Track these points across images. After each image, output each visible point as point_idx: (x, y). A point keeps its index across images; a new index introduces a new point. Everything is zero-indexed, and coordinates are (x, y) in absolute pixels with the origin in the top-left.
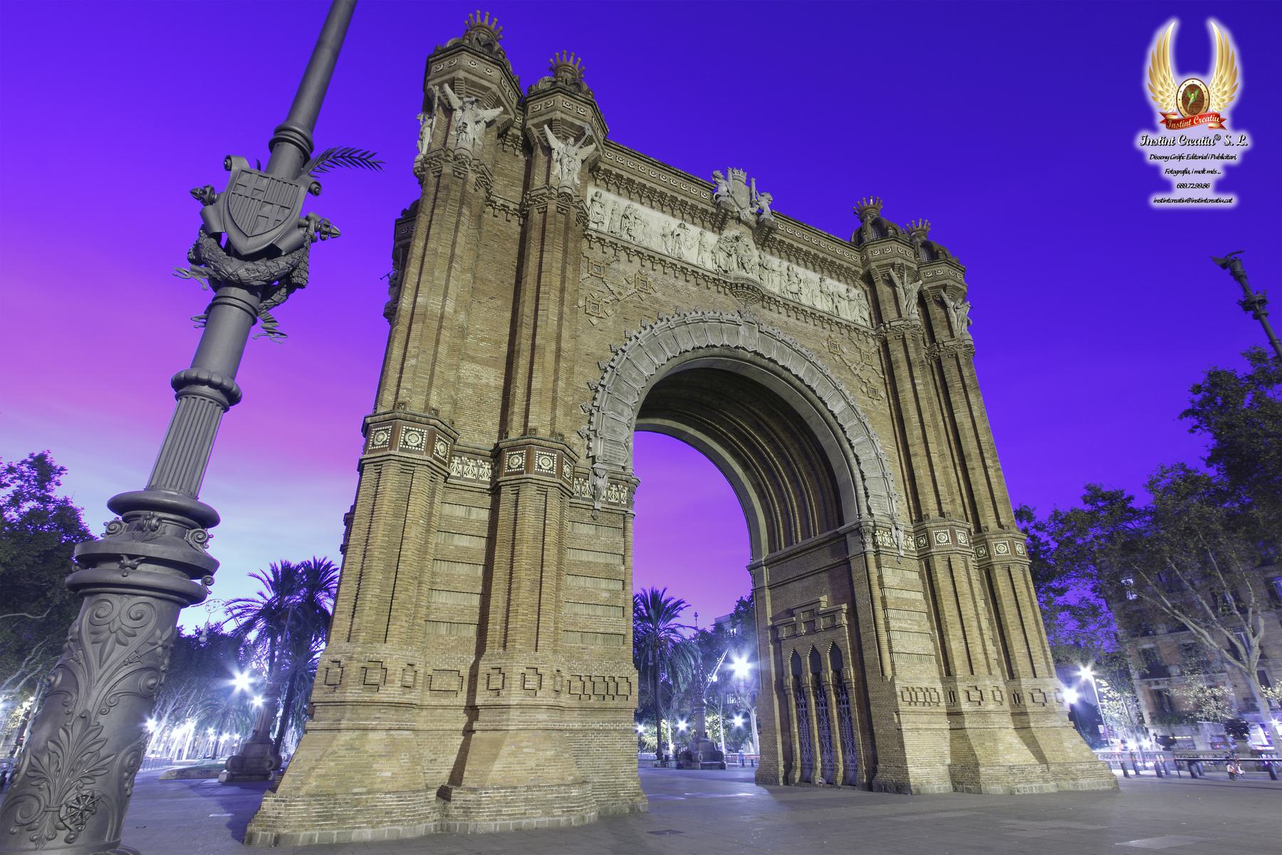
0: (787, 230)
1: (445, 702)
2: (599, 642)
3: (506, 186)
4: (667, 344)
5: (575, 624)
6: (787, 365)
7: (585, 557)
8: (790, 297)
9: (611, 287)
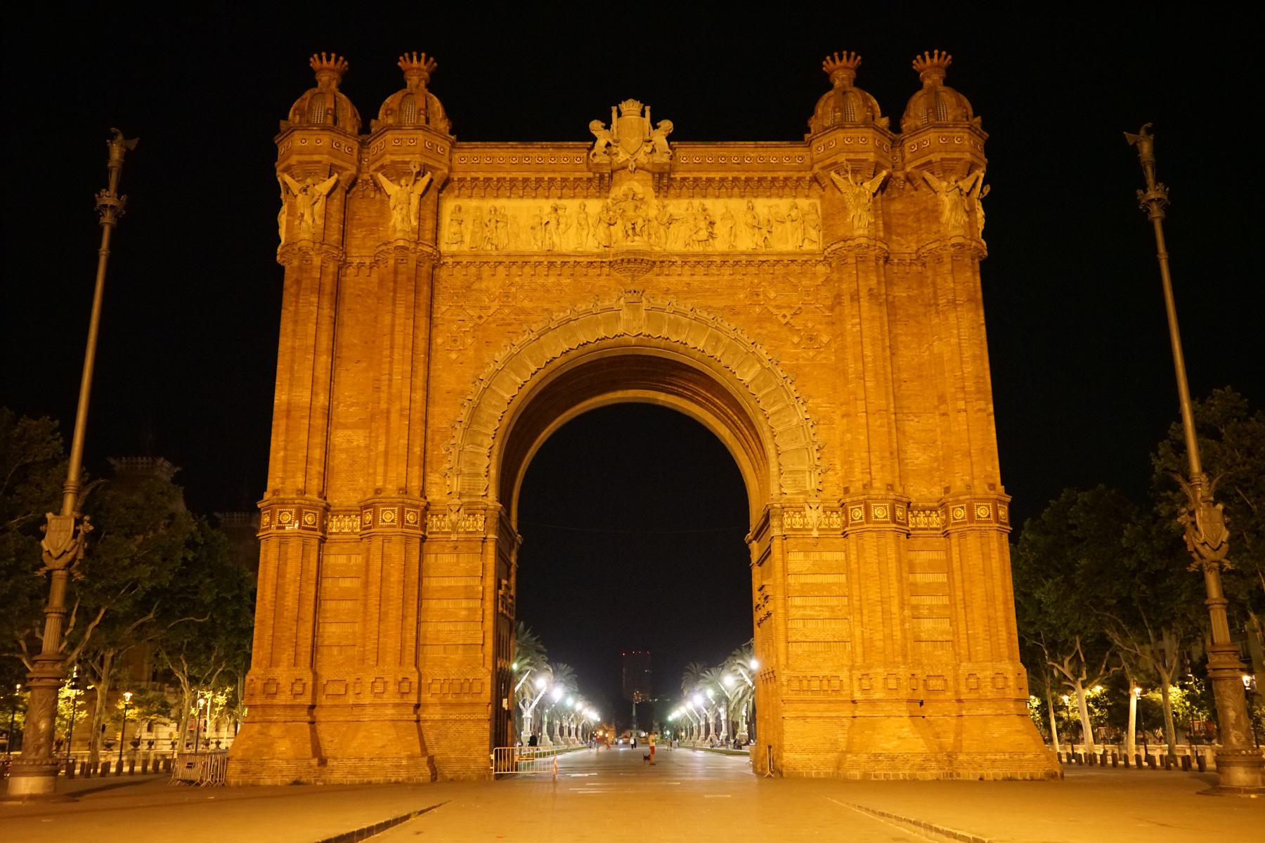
0: (696, 156)
1: (337, 702)
2: (460, 652)
3: (364, 237)
4: (531, 358)
5: (437, 639)
6: (682, 338)
7: (447, 582)
8: (698, 248)
9: (471, 313)
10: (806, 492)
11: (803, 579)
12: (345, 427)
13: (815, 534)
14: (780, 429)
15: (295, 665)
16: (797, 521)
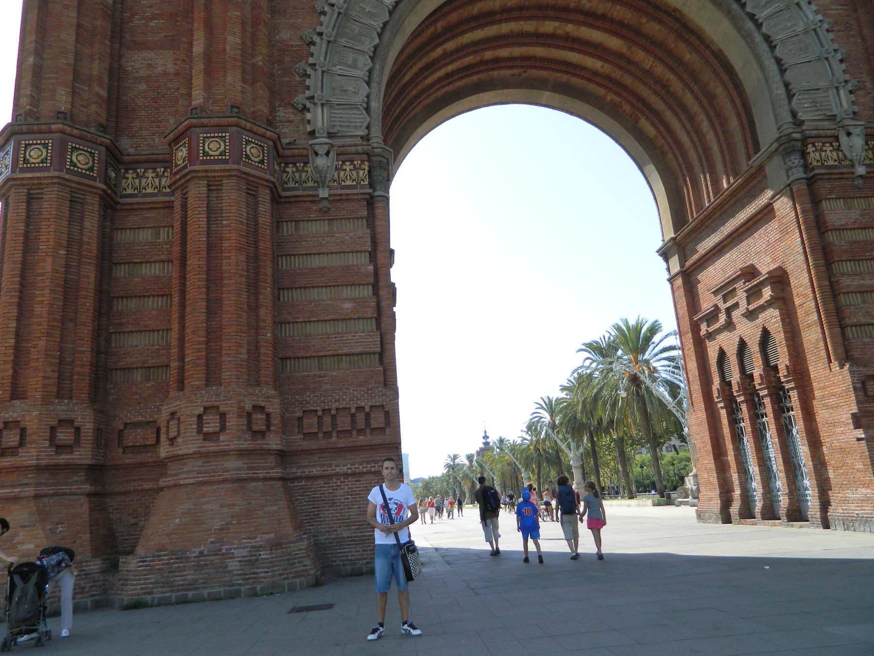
7: (316, 262)
10: (833, 118)
11: (849, 236)
12: (143, 46)
13: (861, 170)
14: (781, 36)
15: (59, 395)
16: (830, 155)
